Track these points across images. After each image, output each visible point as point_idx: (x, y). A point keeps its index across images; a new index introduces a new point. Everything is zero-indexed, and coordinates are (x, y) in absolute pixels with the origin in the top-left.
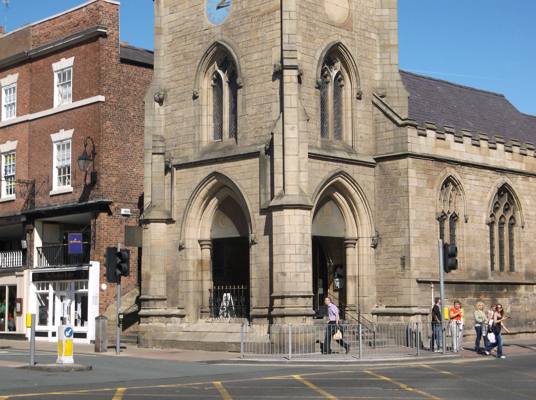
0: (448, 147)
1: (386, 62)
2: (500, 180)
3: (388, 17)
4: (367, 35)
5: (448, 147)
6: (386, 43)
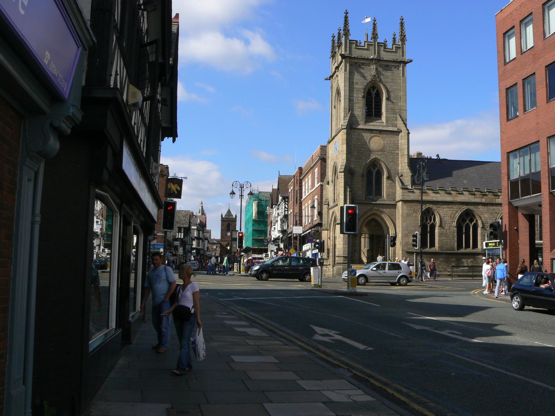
0: (429, 195)
1: (403, 162)
2: (465, 208)
3: (403, 143)
4: (393, 152)
5: (429, 195)
6: (403, 154)
